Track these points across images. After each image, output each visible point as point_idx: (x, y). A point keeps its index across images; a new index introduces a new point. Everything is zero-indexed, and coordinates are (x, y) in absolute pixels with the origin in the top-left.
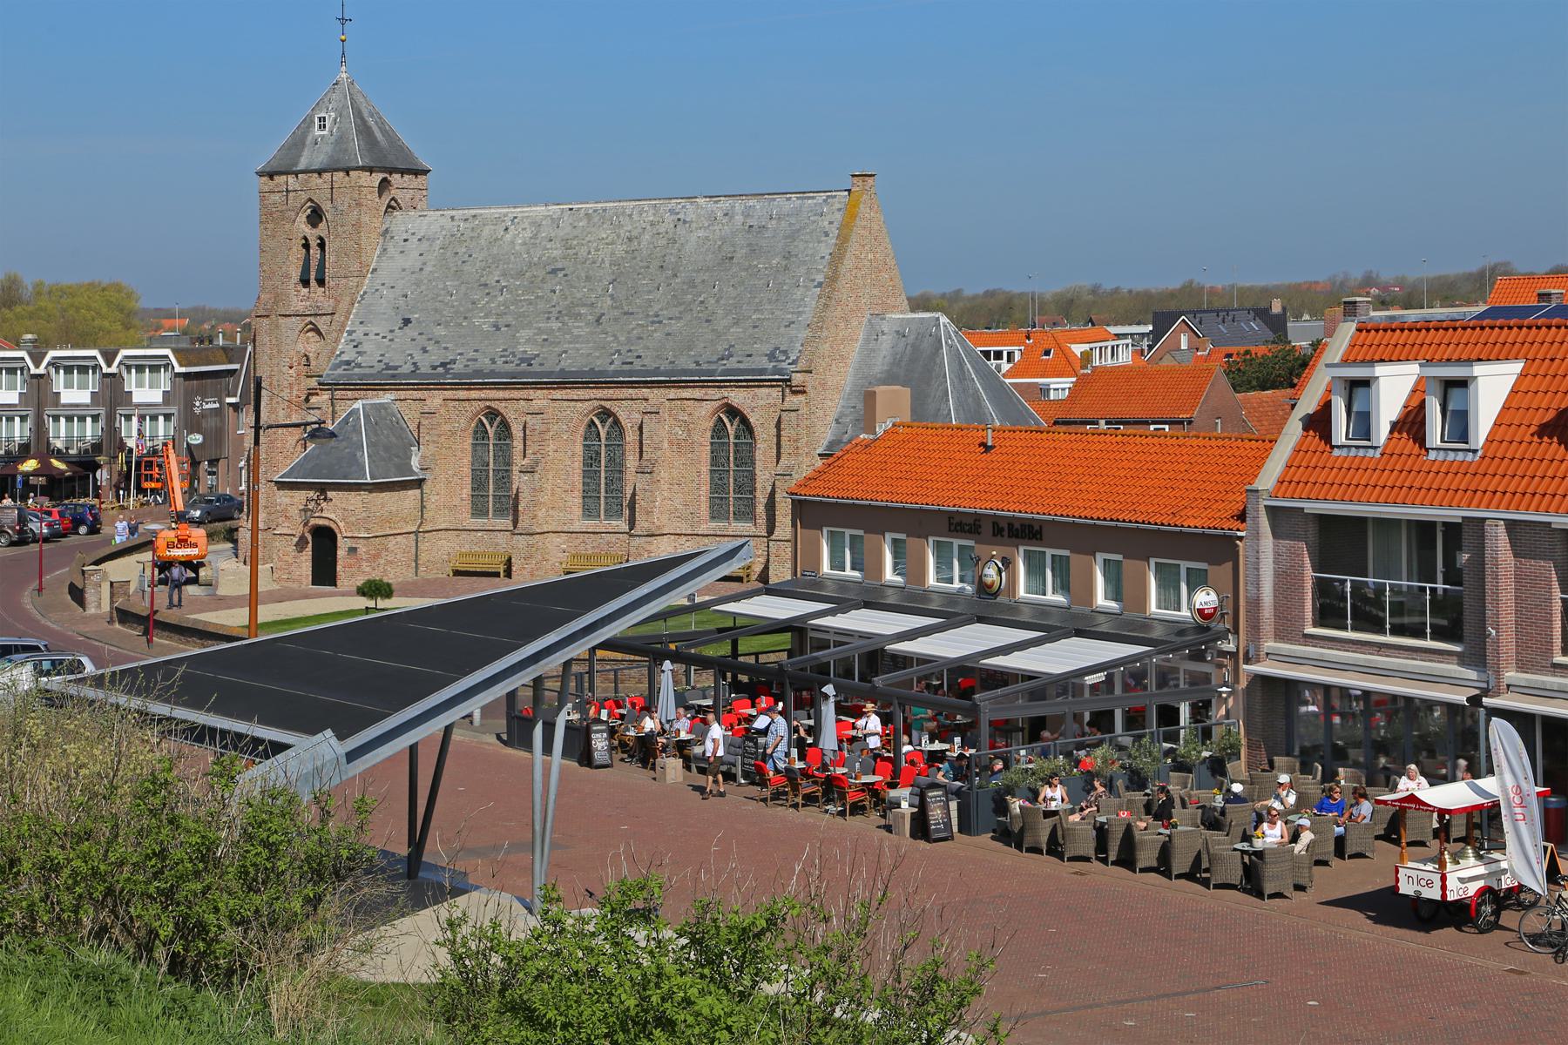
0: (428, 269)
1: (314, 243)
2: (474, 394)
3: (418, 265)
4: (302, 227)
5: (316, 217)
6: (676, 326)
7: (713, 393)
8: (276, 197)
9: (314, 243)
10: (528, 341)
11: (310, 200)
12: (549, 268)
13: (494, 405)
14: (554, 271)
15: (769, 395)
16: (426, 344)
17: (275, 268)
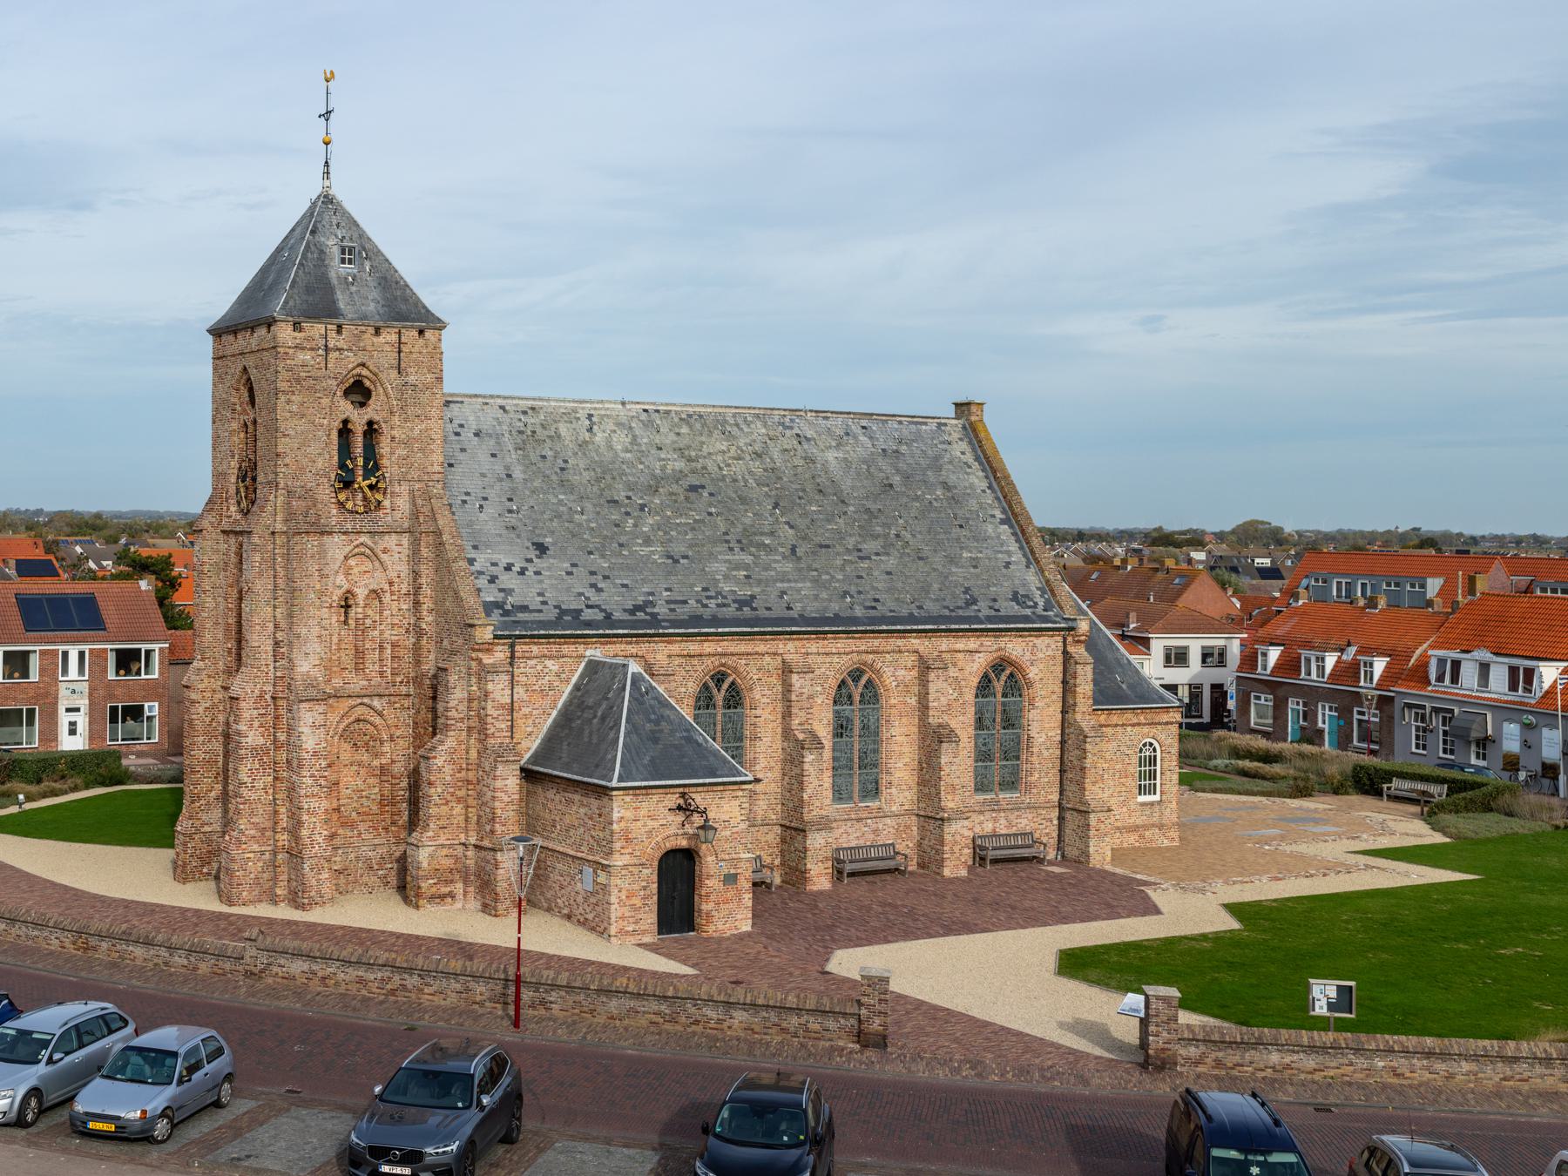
0: (518, 474)
1: (359, 428)
2: (709, 647)
3: (499, 469)
4: (346, 408)
5: (359, 391)
6: (891, 562)
7: (988, 642)
8: (306, 357)
9: (359, 428)
10: (726, 577)
11: (363, 365)
12: (685, 483)
13: (730, 661)
14: (693, 489)
15: (1048, 646)
16: (593, 579)
17: (305, 461)
